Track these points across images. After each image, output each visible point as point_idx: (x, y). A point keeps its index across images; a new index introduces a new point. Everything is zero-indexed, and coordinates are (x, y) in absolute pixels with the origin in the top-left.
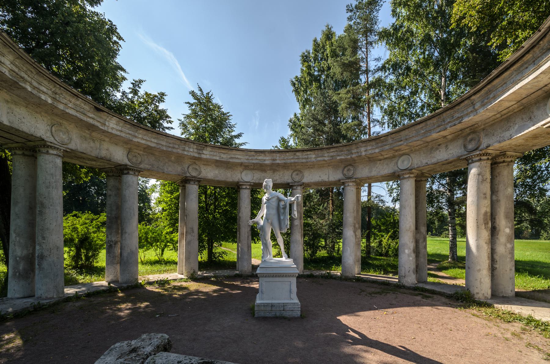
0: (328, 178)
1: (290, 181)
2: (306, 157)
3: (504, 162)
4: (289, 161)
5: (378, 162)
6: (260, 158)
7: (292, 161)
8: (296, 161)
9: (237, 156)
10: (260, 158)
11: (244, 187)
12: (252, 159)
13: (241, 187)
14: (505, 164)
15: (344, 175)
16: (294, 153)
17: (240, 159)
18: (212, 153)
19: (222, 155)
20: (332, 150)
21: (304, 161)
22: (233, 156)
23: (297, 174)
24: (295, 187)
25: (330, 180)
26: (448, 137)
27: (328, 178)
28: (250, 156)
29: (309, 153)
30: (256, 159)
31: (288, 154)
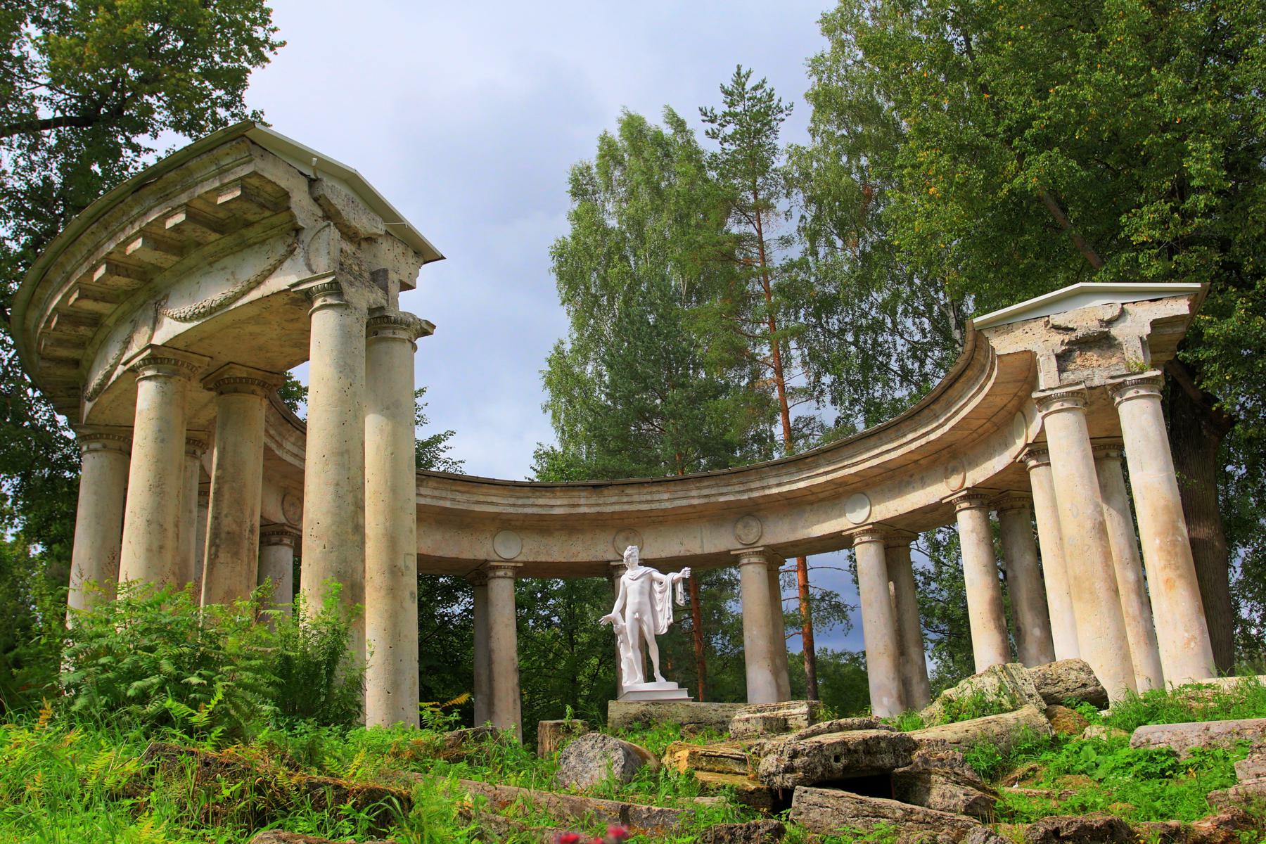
0: (702, 547)
2: (649, 498)
3: (1012, 508)
5: (808, 508)
6: (541, 501)
7: (617, 508)
8: (626, 507)
9: (489, 499)
10: (541, 501)
11: (501, 573)
12: (524, 506)
13: (491, 575)
14: (1014, 511)
15: (738, 538)
16: (621, 488)
17: (497, 504)
18: (437, 493)
19: (459, 497)
20: (706, 483)
22: (482, 498)
25: (707, 551)
27: (702, 547)
28: (518, 498)
29: (655, 489)
30: (533, 505)
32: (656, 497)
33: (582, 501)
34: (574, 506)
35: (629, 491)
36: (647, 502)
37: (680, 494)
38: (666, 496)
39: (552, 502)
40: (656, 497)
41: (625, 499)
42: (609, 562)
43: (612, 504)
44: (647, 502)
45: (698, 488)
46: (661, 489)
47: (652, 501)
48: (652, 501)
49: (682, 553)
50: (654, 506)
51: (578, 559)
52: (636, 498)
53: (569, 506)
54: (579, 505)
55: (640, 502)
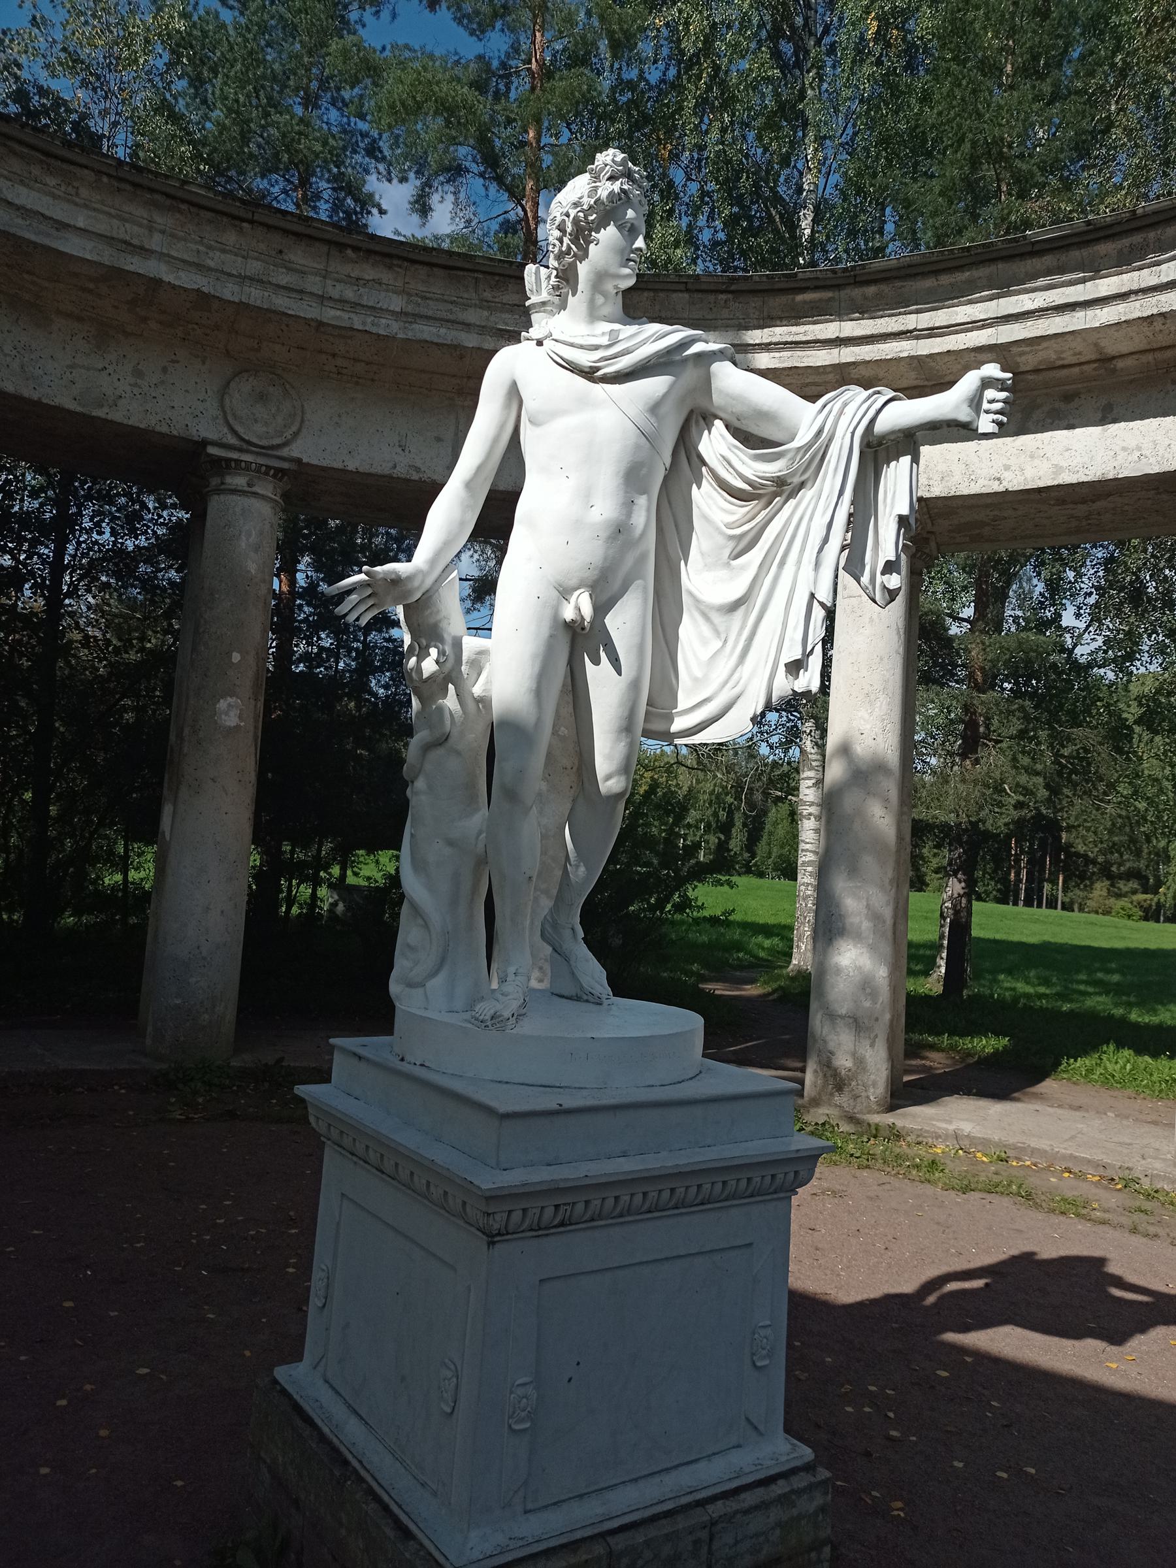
1: (206, 429)
2: (349, 294)
4: (229, 291)
7: (255, 296)
8: (282, 302)
21: (330, 315)
23: (262, 398)
24: (239, 481)
26: (1120, 364)
29: (369, 272)
31: (231, 238)
32: (369, 297)
33: (155, 242)
34: (129, 247)
35: (298, 256)
36: (341, 302)
37: (431, 308)
38: (396, 303)
39: (59, 211)
40: (369, 297)
41: (284, 279)
42: (205, 443)
43: (242, 279)
44: (341, 302)
45: (484, 304)
46: (386, 276)
47: (355, 306)
48: (355, 306)
49: (401, 471)
50: (357, 321)
51: (117, 416)
52: (313, 284)
53: (109, 240)
54: (143, 251)
55: (322, 299)
